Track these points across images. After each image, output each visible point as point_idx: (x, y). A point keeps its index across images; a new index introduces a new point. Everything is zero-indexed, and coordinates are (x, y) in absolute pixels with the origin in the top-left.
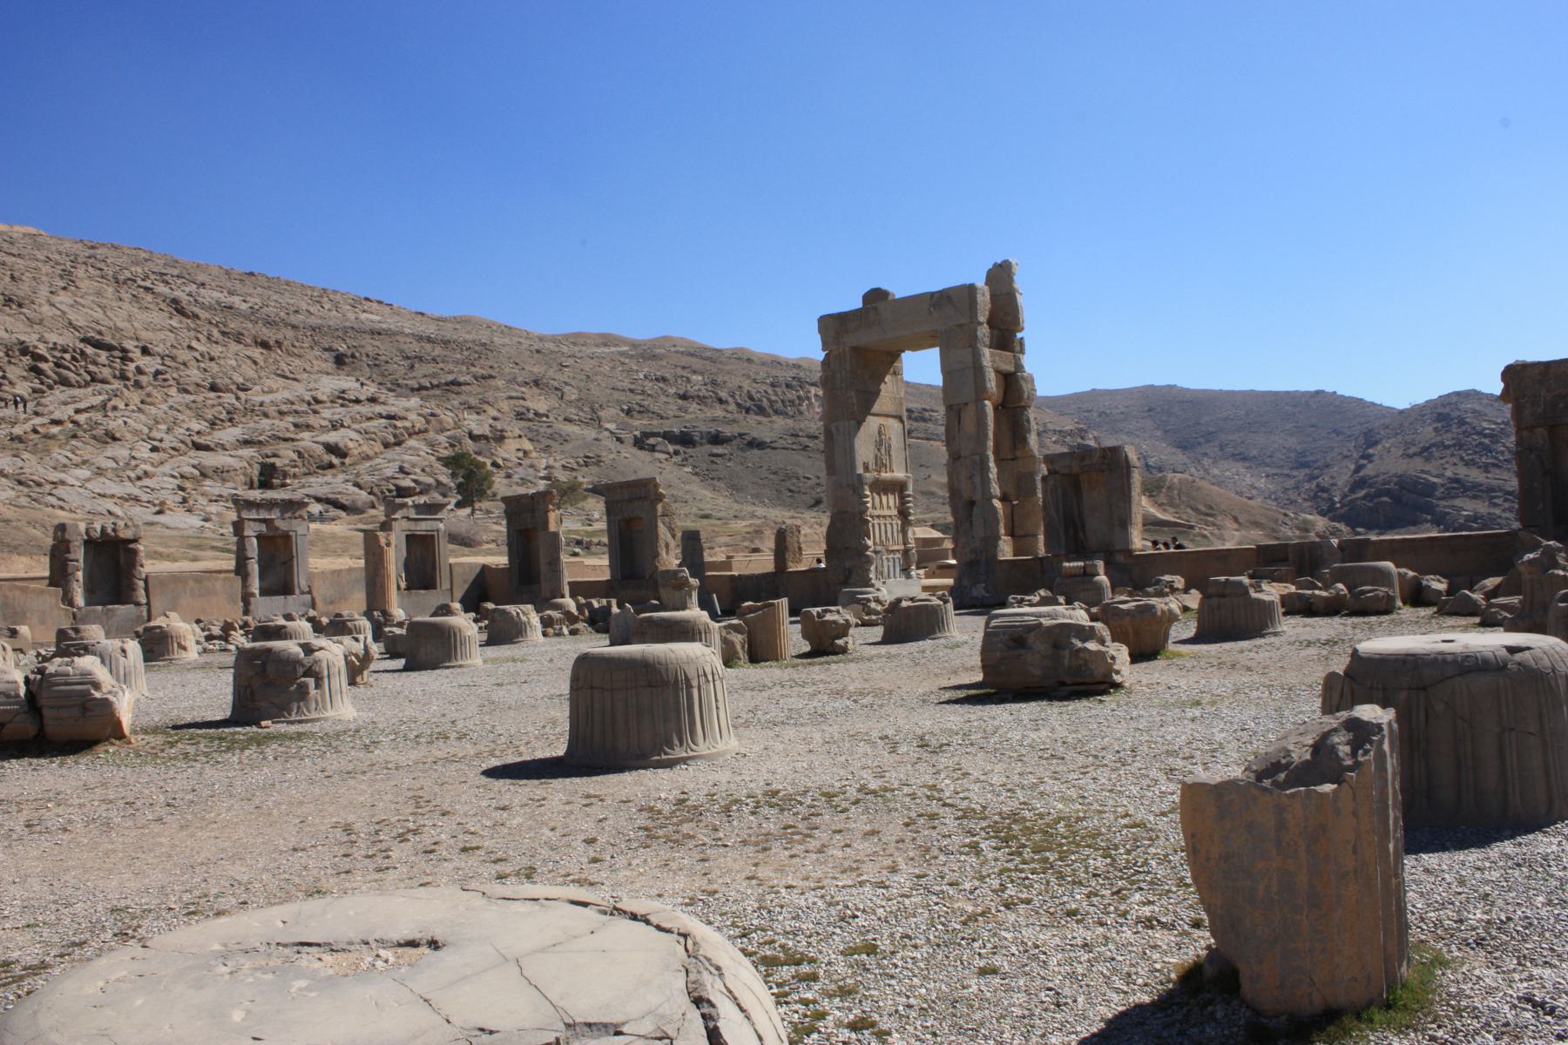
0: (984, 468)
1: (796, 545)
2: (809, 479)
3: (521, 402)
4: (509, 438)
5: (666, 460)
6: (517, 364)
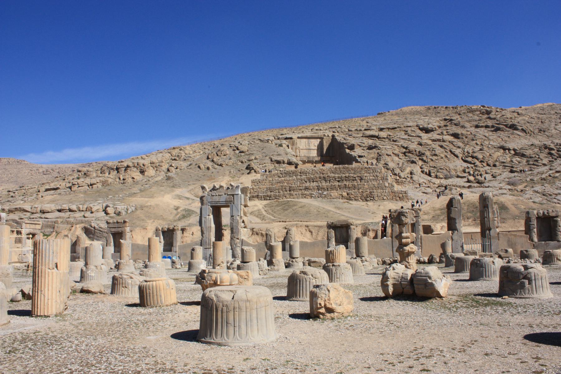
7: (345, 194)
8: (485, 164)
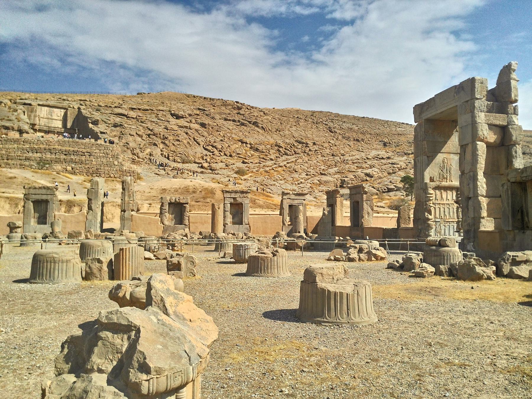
0: (474, 178)
1: (407, 216)
7: (69, 168)
8: (222, 154)
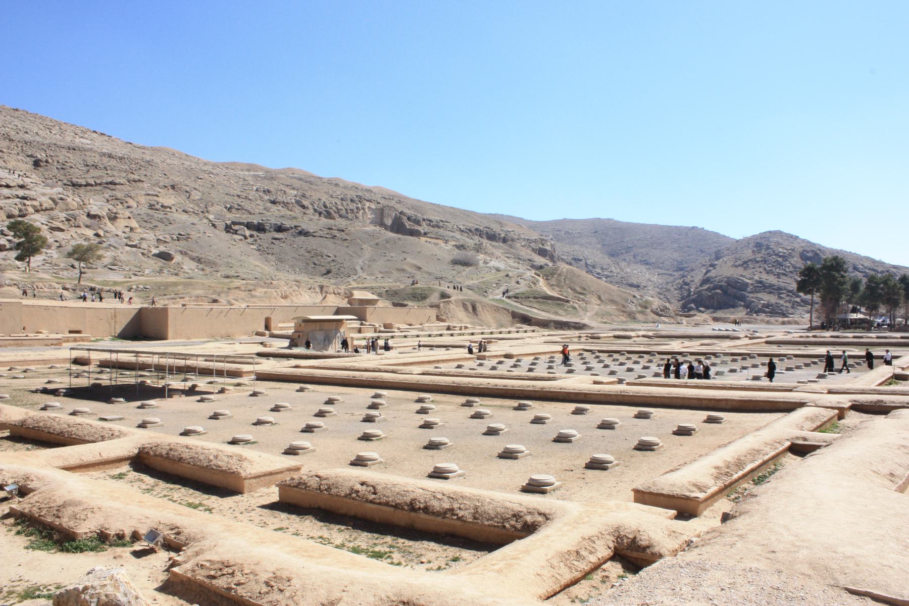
2: (329, 257)
3: (155, 198)
4: (120, 218)
5: (241, 240)
6: (165, 175)
